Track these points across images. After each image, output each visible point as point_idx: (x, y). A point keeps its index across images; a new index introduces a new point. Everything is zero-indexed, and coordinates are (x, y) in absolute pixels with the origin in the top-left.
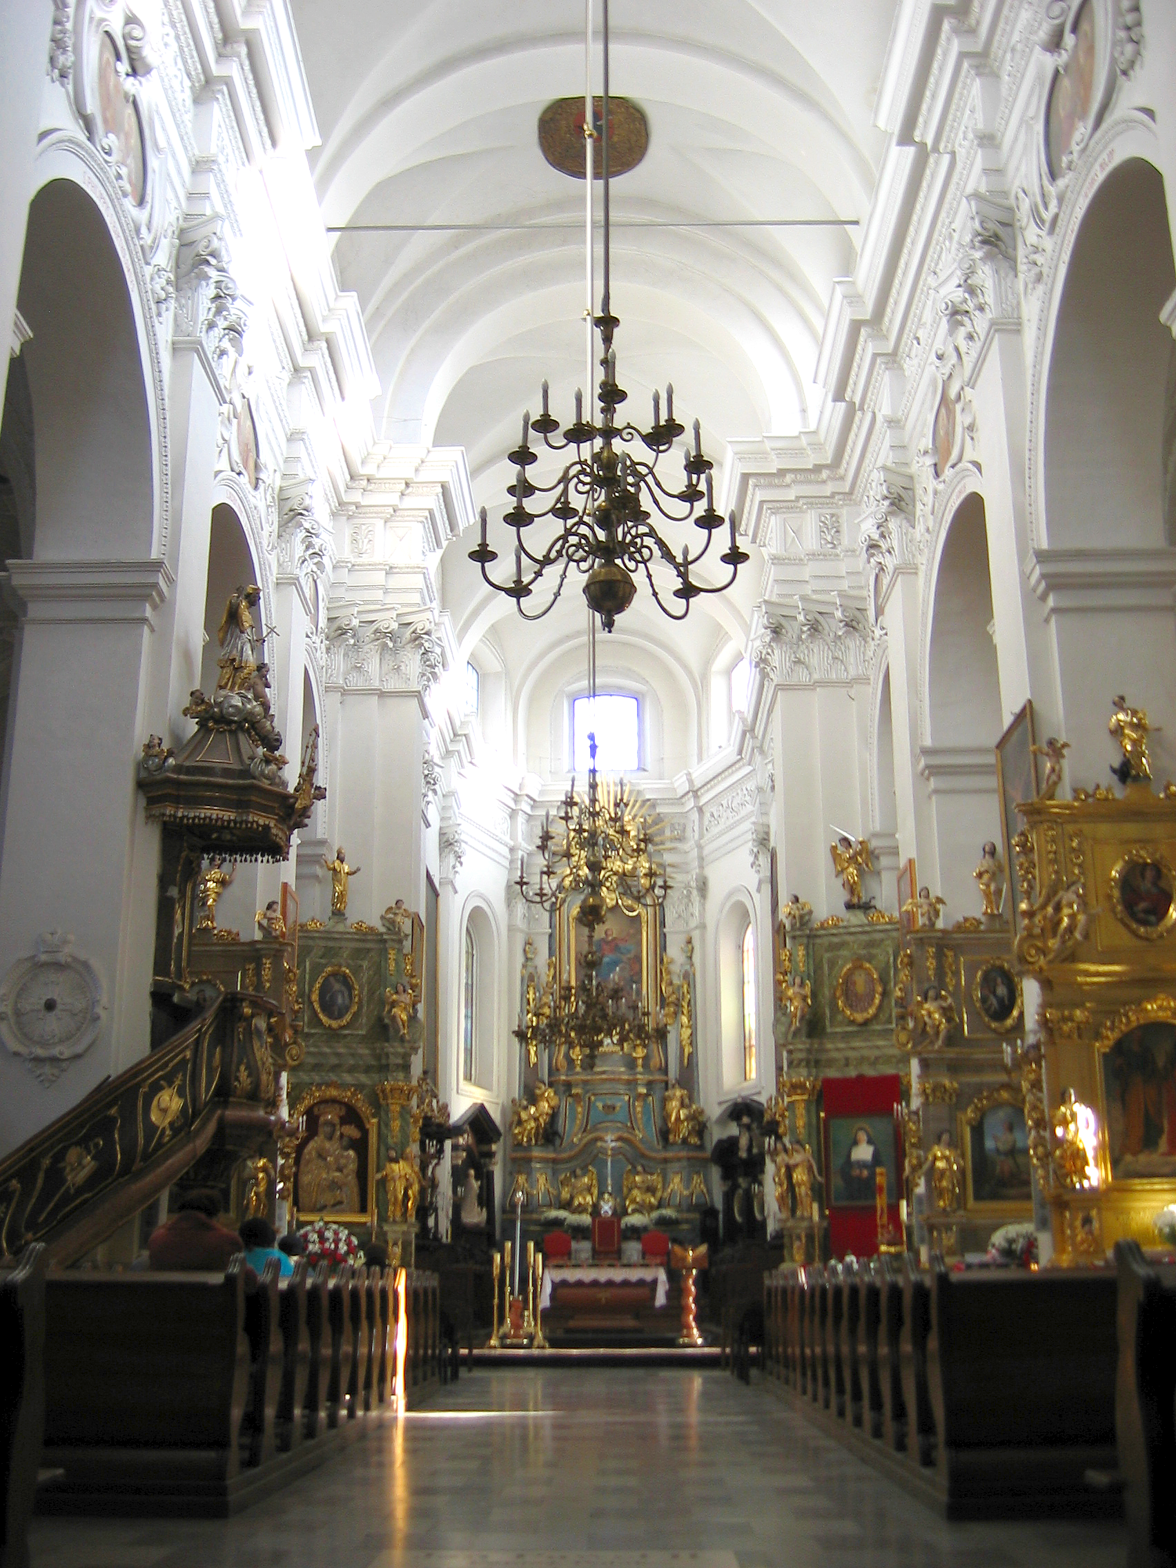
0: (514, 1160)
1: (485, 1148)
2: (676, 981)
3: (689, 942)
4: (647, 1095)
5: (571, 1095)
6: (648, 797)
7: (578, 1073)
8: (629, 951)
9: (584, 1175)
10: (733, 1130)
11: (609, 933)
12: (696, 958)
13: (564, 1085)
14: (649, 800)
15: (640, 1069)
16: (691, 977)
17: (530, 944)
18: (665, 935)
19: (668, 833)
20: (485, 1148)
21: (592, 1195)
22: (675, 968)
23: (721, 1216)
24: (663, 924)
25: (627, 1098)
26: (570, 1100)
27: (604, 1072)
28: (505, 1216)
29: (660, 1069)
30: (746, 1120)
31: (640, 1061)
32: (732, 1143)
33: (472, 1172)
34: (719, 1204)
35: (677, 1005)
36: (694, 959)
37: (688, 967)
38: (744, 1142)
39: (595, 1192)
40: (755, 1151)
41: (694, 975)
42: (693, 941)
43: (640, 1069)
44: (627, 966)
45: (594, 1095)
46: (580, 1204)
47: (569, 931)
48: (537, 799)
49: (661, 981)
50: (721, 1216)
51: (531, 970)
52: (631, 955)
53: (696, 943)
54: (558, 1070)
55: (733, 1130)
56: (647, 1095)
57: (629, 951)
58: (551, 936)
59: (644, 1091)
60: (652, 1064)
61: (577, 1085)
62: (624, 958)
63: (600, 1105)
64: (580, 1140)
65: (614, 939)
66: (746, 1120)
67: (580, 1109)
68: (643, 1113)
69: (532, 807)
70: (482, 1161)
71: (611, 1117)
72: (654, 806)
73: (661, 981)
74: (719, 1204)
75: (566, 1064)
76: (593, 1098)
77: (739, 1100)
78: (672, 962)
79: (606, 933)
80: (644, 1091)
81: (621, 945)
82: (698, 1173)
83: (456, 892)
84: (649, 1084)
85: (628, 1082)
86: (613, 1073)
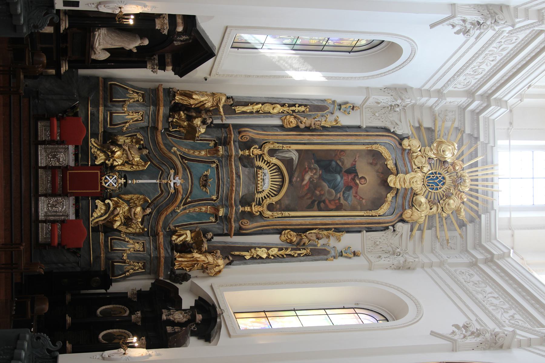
0: (155, 91)
1: (169, 59)
2: (321, 242)
3: (355, 254)
4: (216, 217)
5: (216, 145)
6: (483, 216)
7: (237, 151)
8: (346, 199)
9: (141, 158)
10: (188, 302)
11: (363, 180)
12: (341, 261)
13: (225, 138)
14: (480, 217)
15: (241, 209)
16: (325, 257)
17: (353, 109)
18: (360, 232)
19: (448, 234)
20: (169, 59)
21: (123, 164)
22: (332, 242)
23: (103, 291)
24: (369, 230)
25: (214, 197)
26: (212, 144)
27: (238, 176)
28: (100, 79)
29: (241, 228)
30: (199, 317)
31: (248, 209)
32: (177, 303)
33: (146, 42)
34: (117, 287)
35: (298, 244)
36: (341, 259)
37: (333, 253)
38: (178, 317)
39: (127, 168)
40: (169, 329)
41: (326, 260)
42: (356, 258)
43: (241, 209)
44: (333, 198)
45: (217, 167)
46: (113, 152)
47: (364, 144)
48: (481, 116)
49: (320, 229)
50: (103, 291)
51: (331, 108)
52: (342, 201)
53: (355, 261)
54: (240, 133)
55: (188, 302)
56: (216, 217)
57: (346, 199)
58: (359, 127)
59: (221, 213)
60: (245, 221)
61: (226, 150)
62: (341, 195)
63: (208, 173)
64: (175, 153)
65: (357, 185)
66: (199, 317)
67: (203, 153)
68: (200, 213)
69: (473, 111)
70: (156, 57)
71: (196, 182)
72: (472, 221)
73: (320, 229)
74: (117, 287)
75: (245, 140)
76: (214, 165)
77: (218, 309)
78: (339, 240)
79: (363, 178)
80: (221, 213)
81: (353, 192)
82: (144, 267)
83: (432, 26)
84: (226, 219)
85: (228, 198)
86: (238, 185)
